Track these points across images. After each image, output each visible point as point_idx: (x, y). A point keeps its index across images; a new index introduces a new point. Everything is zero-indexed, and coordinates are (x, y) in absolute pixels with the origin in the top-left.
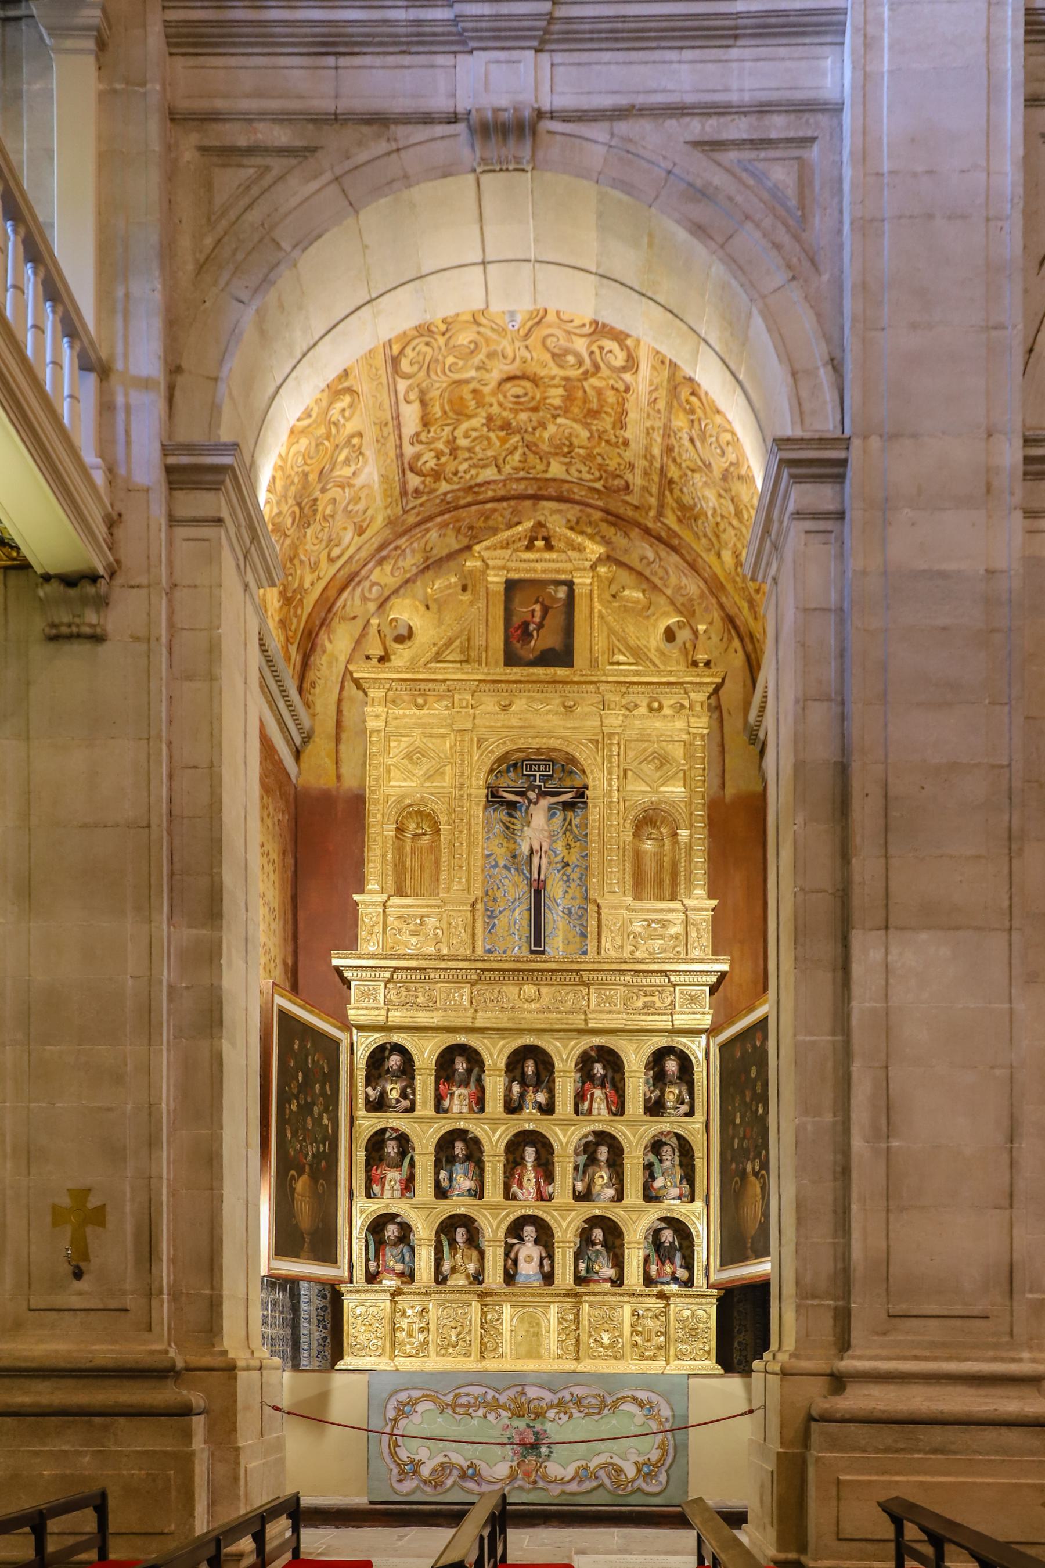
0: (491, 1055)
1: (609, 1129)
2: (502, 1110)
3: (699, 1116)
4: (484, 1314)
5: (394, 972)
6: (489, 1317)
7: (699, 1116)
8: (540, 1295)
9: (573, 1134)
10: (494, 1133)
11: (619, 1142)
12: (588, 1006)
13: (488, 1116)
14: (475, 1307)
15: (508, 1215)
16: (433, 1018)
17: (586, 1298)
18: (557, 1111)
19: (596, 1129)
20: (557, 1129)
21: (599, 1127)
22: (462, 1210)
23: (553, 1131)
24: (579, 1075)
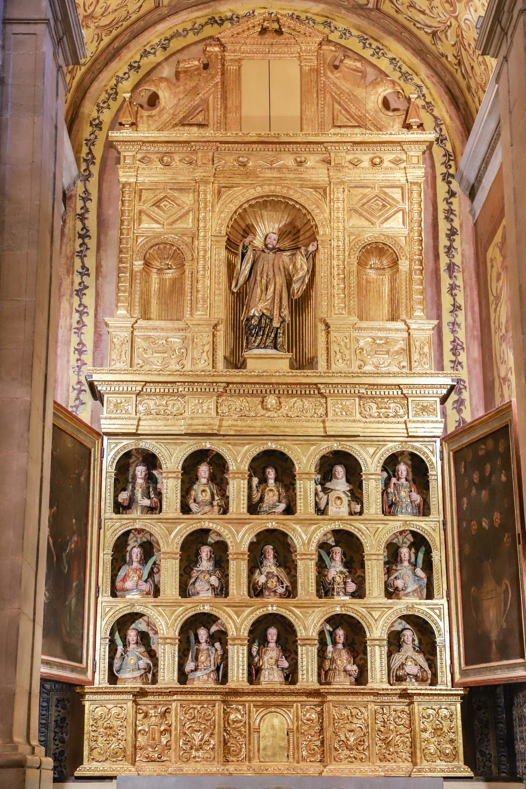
0: (236, 460)
1: (348, 528)
2: (245, 510)
3: (436, 516)
4: (226, 713)
5: (144, 386)
6: (232, 717)
7: (436, 516)
8: (282, 694)
9: (314, 532)
10: (238, 532)
11: (358, 539)
12: (326, 414)
13: (234, 516)
14: (219, 707)
15: (251, 613)
16: (180, 427)
17: (330, 698)
18: (298, 511)
19: (337, 527)
20: (298, 527)
21: (337, 526)
22: (207, 609)
23: (294, 530)
24: (319, 476)
